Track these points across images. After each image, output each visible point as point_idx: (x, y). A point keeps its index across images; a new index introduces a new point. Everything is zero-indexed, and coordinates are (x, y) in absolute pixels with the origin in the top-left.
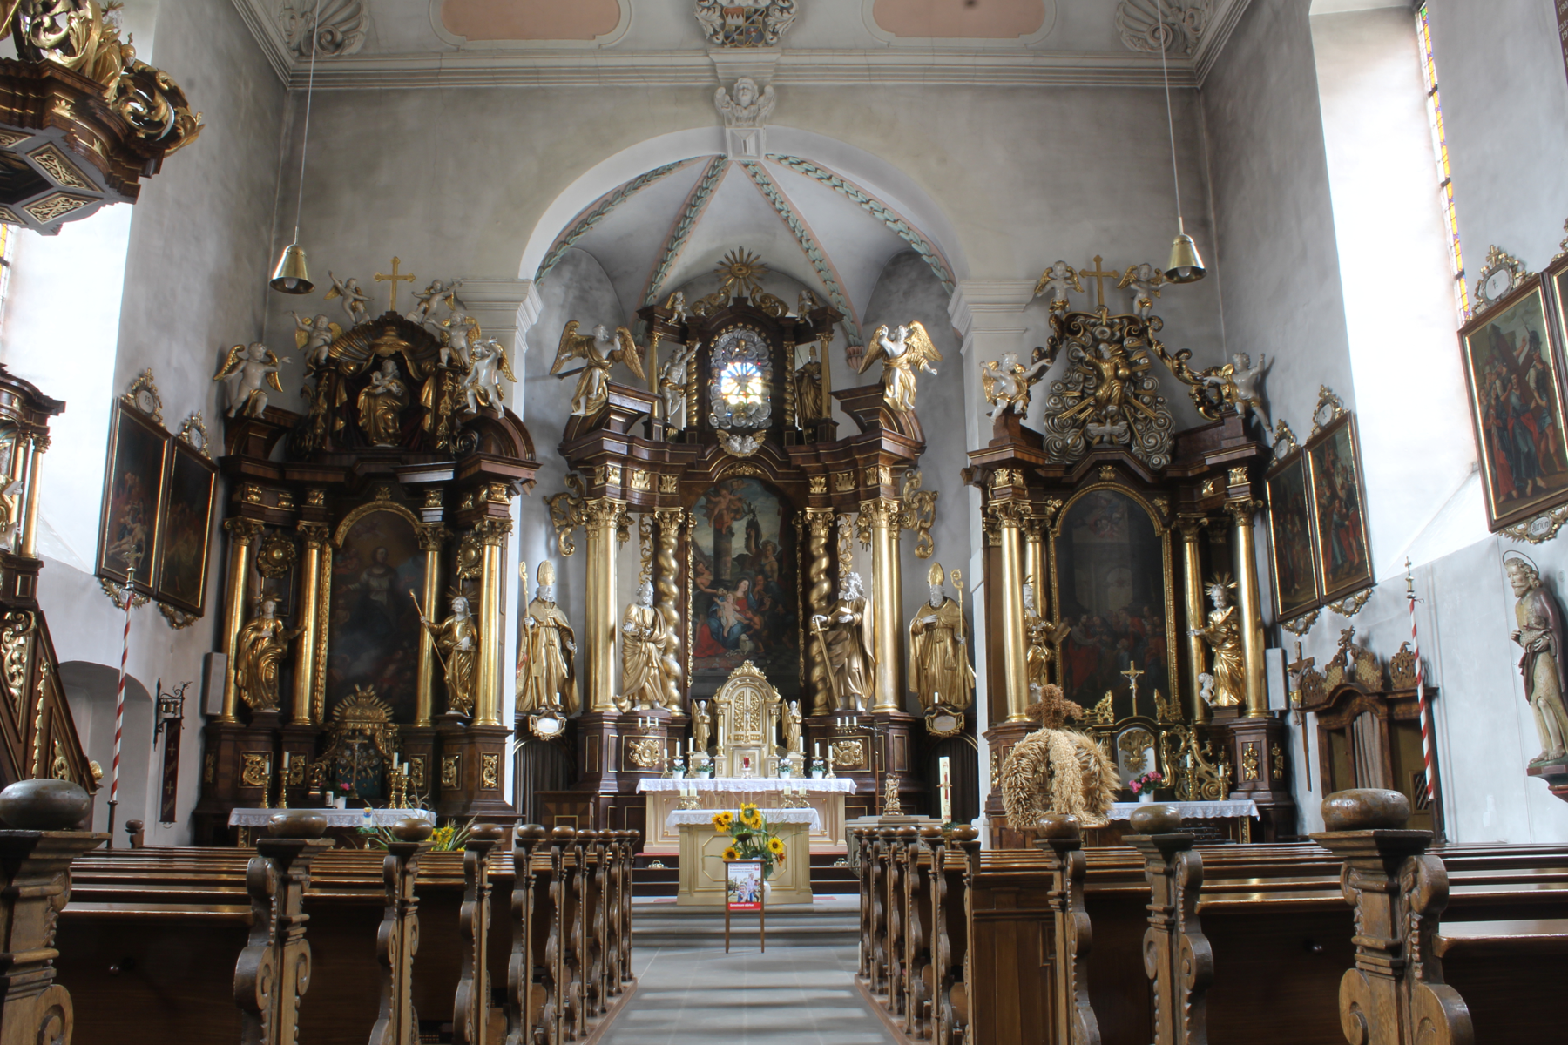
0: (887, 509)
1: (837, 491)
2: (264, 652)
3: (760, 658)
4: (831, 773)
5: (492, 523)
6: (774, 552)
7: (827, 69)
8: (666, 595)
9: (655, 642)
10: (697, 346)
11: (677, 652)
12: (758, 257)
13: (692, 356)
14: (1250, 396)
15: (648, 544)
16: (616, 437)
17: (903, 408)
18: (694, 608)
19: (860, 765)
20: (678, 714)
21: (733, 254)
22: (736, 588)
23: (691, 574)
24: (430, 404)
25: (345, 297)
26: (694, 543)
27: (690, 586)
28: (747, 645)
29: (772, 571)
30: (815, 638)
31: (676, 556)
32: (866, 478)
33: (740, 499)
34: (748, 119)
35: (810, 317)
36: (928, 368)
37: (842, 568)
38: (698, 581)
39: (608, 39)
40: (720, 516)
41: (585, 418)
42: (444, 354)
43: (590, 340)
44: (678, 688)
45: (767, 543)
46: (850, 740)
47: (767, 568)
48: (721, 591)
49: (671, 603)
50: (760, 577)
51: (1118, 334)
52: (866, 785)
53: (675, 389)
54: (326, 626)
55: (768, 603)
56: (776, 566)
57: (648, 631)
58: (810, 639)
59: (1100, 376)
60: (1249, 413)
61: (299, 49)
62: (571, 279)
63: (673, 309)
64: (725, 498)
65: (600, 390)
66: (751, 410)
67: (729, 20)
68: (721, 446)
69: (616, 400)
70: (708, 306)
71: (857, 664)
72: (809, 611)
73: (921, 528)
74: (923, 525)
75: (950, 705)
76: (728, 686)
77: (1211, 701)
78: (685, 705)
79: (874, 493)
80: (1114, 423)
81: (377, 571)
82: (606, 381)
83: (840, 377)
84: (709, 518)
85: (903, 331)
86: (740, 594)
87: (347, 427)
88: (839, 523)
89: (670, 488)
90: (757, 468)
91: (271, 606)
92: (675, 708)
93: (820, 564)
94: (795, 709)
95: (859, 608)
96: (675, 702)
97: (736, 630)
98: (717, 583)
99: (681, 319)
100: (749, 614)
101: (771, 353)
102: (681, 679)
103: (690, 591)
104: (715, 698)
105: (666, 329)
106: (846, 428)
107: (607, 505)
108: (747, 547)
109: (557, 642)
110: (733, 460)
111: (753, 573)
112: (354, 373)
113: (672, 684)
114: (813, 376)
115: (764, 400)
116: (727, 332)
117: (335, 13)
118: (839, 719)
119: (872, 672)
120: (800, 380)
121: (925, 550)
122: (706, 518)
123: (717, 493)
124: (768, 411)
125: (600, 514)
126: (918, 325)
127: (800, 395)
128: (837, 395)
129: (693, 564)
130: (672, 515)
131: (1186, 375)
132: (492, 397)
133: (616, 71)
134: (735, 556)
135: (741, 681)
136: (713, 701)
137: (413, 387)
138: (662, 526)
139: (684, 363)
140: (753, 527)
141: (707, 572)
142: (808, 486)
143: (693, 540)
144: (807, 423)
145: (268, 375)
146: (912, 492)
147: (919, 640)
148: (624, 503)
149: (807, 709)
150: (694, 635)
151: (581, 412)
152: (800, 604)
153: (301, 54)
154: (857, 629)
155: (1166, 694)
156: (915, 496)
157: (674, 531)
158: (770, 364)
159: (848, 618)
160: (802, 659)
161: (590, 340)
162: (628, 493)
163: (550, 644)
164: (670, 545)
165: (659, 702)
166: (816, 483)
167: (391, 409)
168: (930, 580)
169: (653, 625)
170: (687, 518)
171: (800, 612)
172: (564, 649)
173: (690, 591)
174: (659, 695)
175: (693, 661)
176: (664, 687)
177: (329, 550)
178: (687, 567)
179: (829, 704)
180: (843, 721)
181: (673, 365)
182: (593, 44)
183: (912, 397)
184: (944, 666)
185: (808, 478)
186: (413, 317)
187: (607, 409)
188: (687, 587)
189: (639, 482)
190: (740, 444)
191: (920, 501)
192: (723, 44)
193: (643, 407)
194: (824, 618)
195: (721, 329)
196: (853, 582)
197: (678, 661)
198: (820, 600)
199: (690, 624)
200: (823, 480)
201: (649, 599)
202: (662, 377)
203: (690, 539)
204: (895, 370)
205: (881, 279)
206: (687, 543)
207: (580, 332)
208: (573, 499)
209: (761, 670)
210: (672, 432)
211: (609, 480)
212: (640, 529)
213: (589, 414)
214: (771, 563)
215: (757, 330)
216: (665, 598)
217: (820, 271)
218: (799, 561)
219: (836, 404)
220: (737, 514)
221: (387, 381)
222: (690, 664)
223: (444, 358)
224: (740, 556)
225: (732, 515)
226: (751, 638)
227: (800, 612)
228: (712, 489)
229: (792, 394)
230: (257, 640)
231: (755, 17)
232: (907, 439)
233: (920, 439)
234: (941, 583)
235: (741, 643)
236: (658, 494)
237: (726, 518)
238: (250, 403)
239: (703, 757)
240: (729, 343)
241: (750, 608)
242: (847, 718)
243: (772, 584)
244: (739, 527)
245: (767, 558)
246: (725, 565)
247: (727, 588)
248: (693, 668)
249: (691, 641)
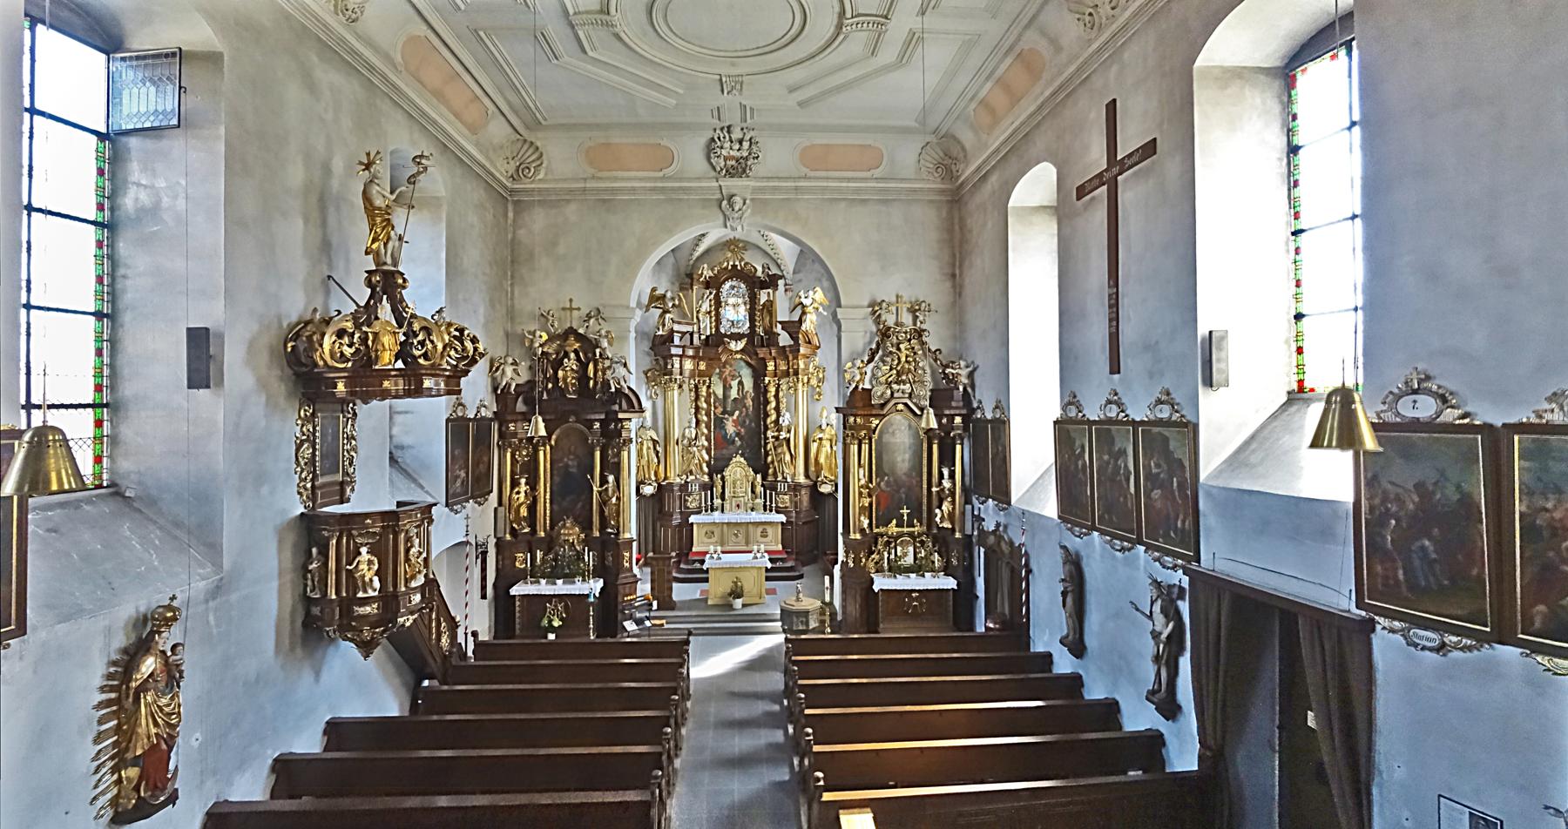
2: (522, 504)
4: (774, 511)
5: (624, 440)
7: (775, 189)
9: (697, 447)
11: (706, 436)
13: (712, 296)
14: (966, 381)
15: (693, 394)
16: (677, 346)
23: (713, 408)
24: (592, 376)
25: (548, 320)
27: (712, 414)
34: (737, 219)
39: (668, 172)
40: (726, 378)
41: (662, 335)
42: (598, 351)
45: (747, 392)
48: (726, 416)
49: (704, 425)
50: (744, 409)
51: (909, 337)
54: (548, 485)
55: (748, 422)
56: (751, 403)
58: (766, 444)
59: (899, 359)
60: (965, 389)
61: (512, 176)
63: (702, 273)
67: (728, 162)
69: (676, 327)
71: (788, 457)
76: (730, 468)
77: (941, 523)
79: (796, 373)
80: (904, 385)
81: (572, 457)
83: (782, 314)
86: (735, 417)
87: (553, 387)
89: (703, 366)
91: (523, 481)
95: (789, 431)
97: (734, 435)
98: (724, 412)
106: (784, 339)
108: (738, 394)
109: (652, 447)
112: (555, 359)
114: (770, 307)
117: (529, 157)
120: (762, 309)
128: (780, 322)
131: (939, 362)
132: (623, 383)
133: (673, 189)
137: (584, 366)
140: (741, 383)
142: (767, 366)
144: (766, 332)
145: (514, 370)
149: (764, 479)
151: (660, 333)
153: (514, 179)
154: (788, 440)
155: (920, 521)
157: (704, 389)
159: (784, 436)
161: (664, 296)
163: (649, 448)
167: (573, 378)
169: (696, 439)
171: (762, 427)
172: (655, 448)
174: (699, 471)
177: (548, 447)
182: (661, 174)
184: (827, 457)
186: (581, 331)
187: (672, 331)
189: (688, 365)
192: (725, 175)
193: (689, 328)
201: (694, 425)
207: (660, 292)
208: (657, 371)
210: (703, 337)
214: (749, 402)
219: (779, 326)
220: (733, 377)
221: (571, 363)
223: (598, 354)
224: (735, 398)
226: (740, 439)
230: (518, 499)
231: (741, 161)
237: (729, 379)
238: (508, 385)
239: (717, 502)
244: (734, 384)
247: (729, 415)
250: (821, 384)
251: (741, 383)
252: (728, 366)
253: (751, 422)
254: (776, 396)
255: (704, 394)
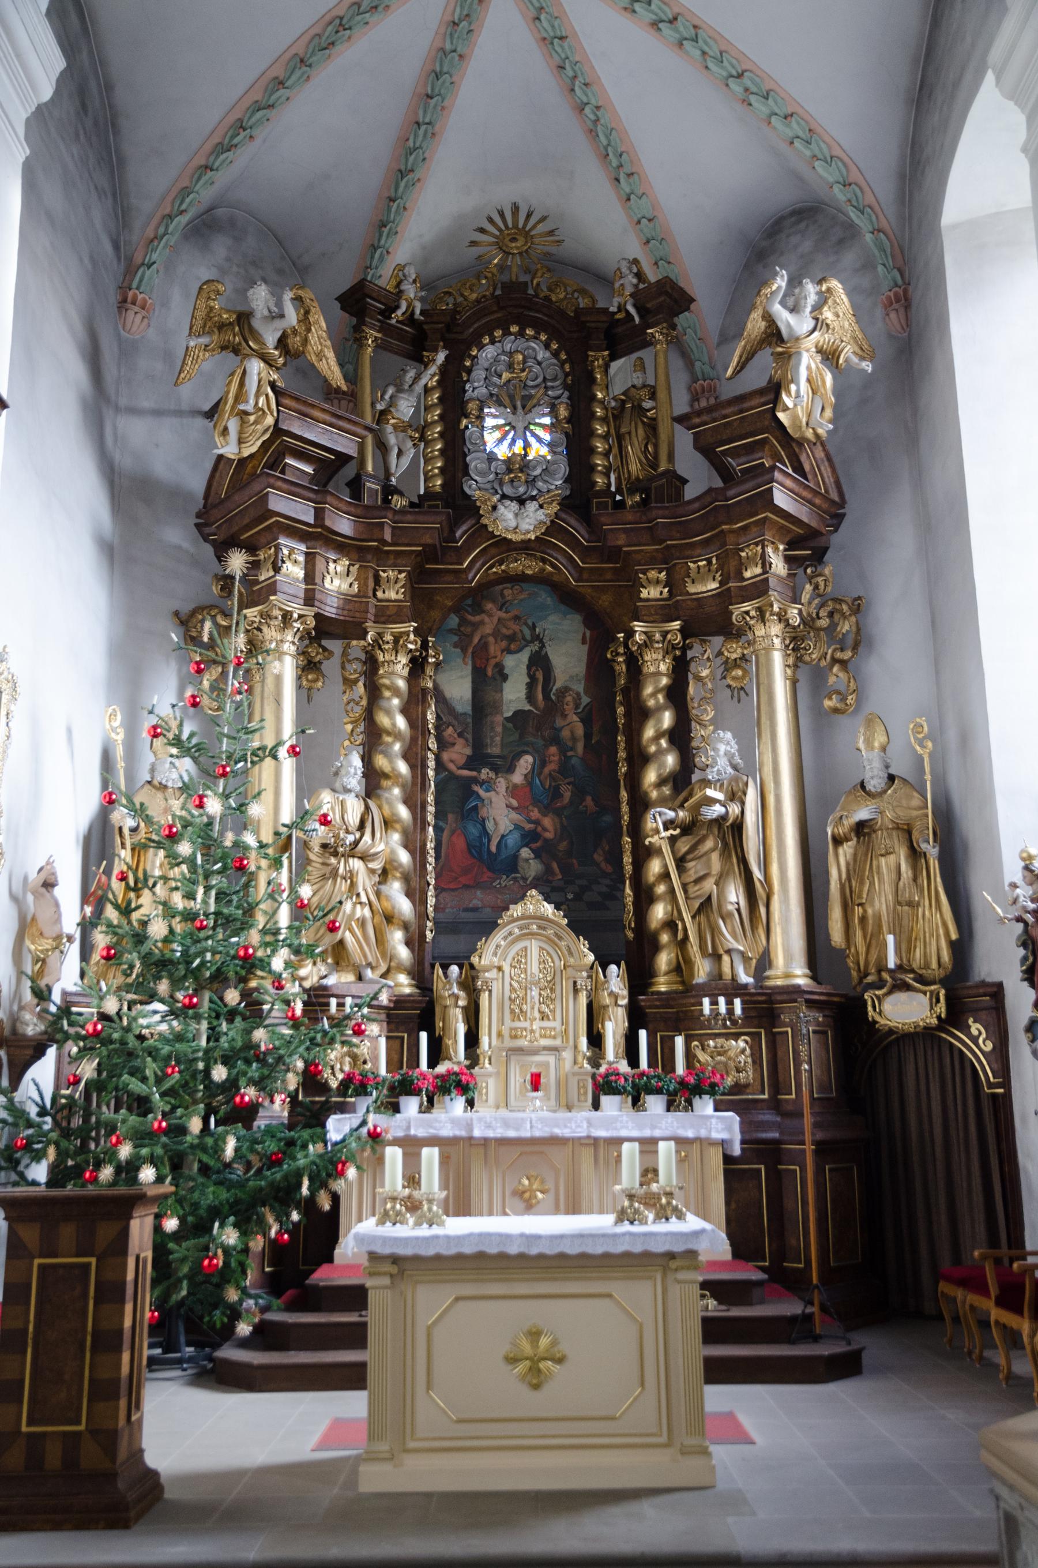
0: (782, 618)
1: (688, 594)
3: (554, 889)
6: (577, 707)
8: (386, 776)
10: (441, 357)
12: (543, 219)
15: (360, 688)
17: (809, 434)
18: (437, 803)
19: (747, 1086)
20: (407, 990)
21: (502, 214)
22: (511, 769)
23: (432, 744)
26: (438, 693)
27: (431, 764)
28: (533, 868)
29: (574, 739)
30: (651, 852)
31: (405, 711)
32: (741, 566)
33: (517, 618)
35: (635, 306)
36: (855, 359)
37: (698, 732)
38: (445, 756)
40: (483, 646)
43: (244, 318)
44: (408, 943)
45: (564, 691)
46: (727, 1036)
47: (565, 733)
48: (485, 773)
49: (396, 791)
50: (553, 749)
52: (762, 1126)
53: (404, 431)
56: (580, 730)
57: (350, 838)
62: (228, 259)
64: (490, 616)
65: (262, 401)
66: (535, 468)
68: (484, 521)
70: (460, 299)
72: (640, 804)
73: (835, 661)
74: (839, 655)
75: (912, 971)
78: (421, 975)
79: (760, 589)
82: (273, 385)
84: (464, 650)
85: (811, 291)
86: (517, 778)
88: (690, 654)
89: (393, 594)
90: (544, 561)
92: (403, 979)
93: (660, 721)
94: (616, 980)
96: (400, 968)
97: (512, 840)
98: (477, 759)
99: (413, 313)
100: (535, 814)
101: (567, 375)
102: (414, 927)
103: (431, 773)
104: (475, 960)
105: (385, 328)
107: (276, 613)
108: (530, 697)
110: (505, 546)
111: (541, 742)
113: (397, 937)
115: (552, 452)
116: (493, 342)
118: (706, 1001)
119: (763, 910)
121: (844, 699)
122: (458, 650)
123: (477, 608)
124: (563, 469)
125: (265, 629)
126: (835, 284)
127: (620, 438)
129: (437, 727)
130: (396, 639)
134: (510, 714)
135: (521, 928)
136: (472, 967)
138: (381, 658)
139: (419, 388)
140: (540, 663)
141: (460, 742)
142: (636, 585)
143: (436, 687)
146: (816, 601)
147: (846, 850)
148: (310, 612)
150: (437, 849)
152: (624, 794)
156: (822, 605)
157: (401, 664)
158: (566, 394)
160: (628, 890)
162: (318, 596)
164: (396, 691)
165: (372, 968)
166: (649, 580)
168: (861, 745)
170: (425, 646)
171: (625, 808)
173: (431, 773)
175: (436, 896)
176: (381, 940)
178: (425, 732)
179: (681, 969)
180: (714, 1003)
181: (400, 390)
183: (829, 413)
185: (637, 572)
188: (424, 766)
190: (516, 515)
191: (831, 615)
194: (671, 814)
195: (482, 336)
196: (722, 748)
197: (409, 894)
198: (661, 783)
199: (431, 829)
200: (663, 575)
202: (380, 407)
203: (430, 685)
204: (799, 354)
205: (746, 266)
206: (424, 690)
209: (558, 908)
211: (284, 570)
212: (343, 668)
213: (246, 453)
214: (572, 726)
215: (543, 337)
216: (385, 783)
217: (648, 242)
218: (621, 721)
220: (512, 643)
222: (431, 901)
224: (518, 713)
225: (504, 644)
226: (537, 854)
227: (625, 808)
228: (469, 601)
229: (606, 437)
232: (816, 493)
233: (834, 496)
234: (884, 749)
235: (521, 864)
236: (373, 601)
240: (496, 360)
241: (536, 802)
242: (722, 1000)
243: (574, 761)
244: (516, 665)
245: (564, 716)
246: (492, 729)
247: (496, 769)
248: (436, 908)
249: (431, 860)
250: (847, 655)
251: (540, 663)
252: (489, 606)
253: (580, 793)
254: (677, 695)
255: (401, 684)
